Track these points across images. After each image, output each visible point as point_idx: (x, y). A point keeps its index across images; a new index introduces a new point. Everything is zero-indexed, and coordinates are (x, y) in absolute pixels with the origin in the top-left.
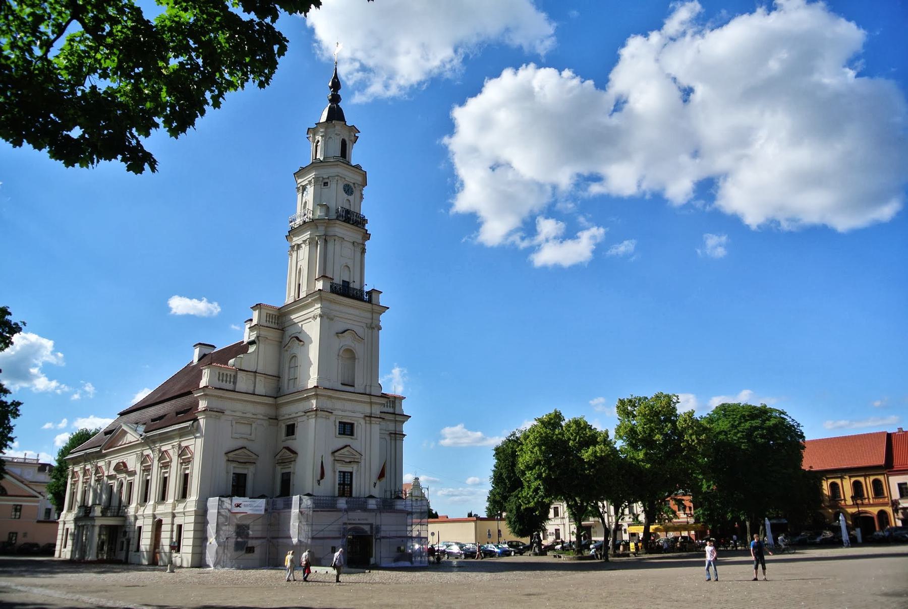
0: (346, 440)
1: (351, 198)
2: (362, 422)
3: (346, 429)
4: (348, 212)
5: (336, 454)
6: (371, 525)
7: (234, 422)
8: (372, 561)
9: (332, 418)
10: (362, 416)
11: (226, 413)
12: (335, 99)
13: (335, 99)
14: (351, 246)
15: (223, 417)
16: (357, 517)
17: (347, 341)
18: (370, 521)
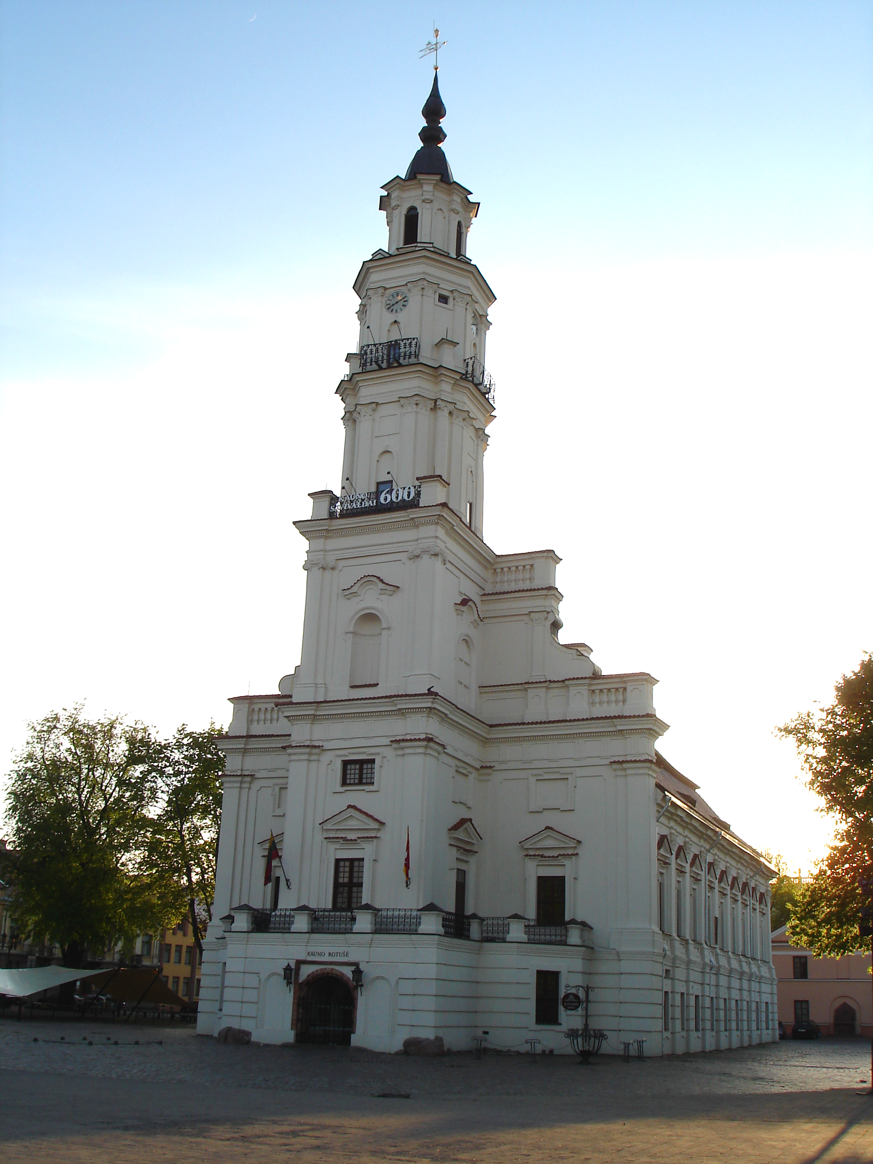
0: (358, 797)
1: (401, 317)
2: (389, 752)
3: (357, 771)
4: (393, 346)
5: (328, 826)
6: (356, 964)
7: (277, 789)
8: (356, 1040)
9: (326, 757)
10: (387, 741)
11: (258, 775)
12: (432, 135)
13: (432, 135)
14: (394, 409)
15: (256, 785)
16: (330, 950)
17: (371, 599)
18: (351, 959)
